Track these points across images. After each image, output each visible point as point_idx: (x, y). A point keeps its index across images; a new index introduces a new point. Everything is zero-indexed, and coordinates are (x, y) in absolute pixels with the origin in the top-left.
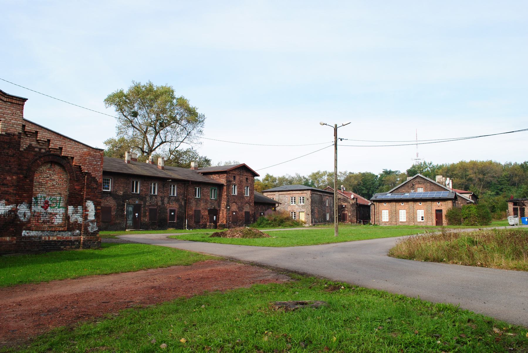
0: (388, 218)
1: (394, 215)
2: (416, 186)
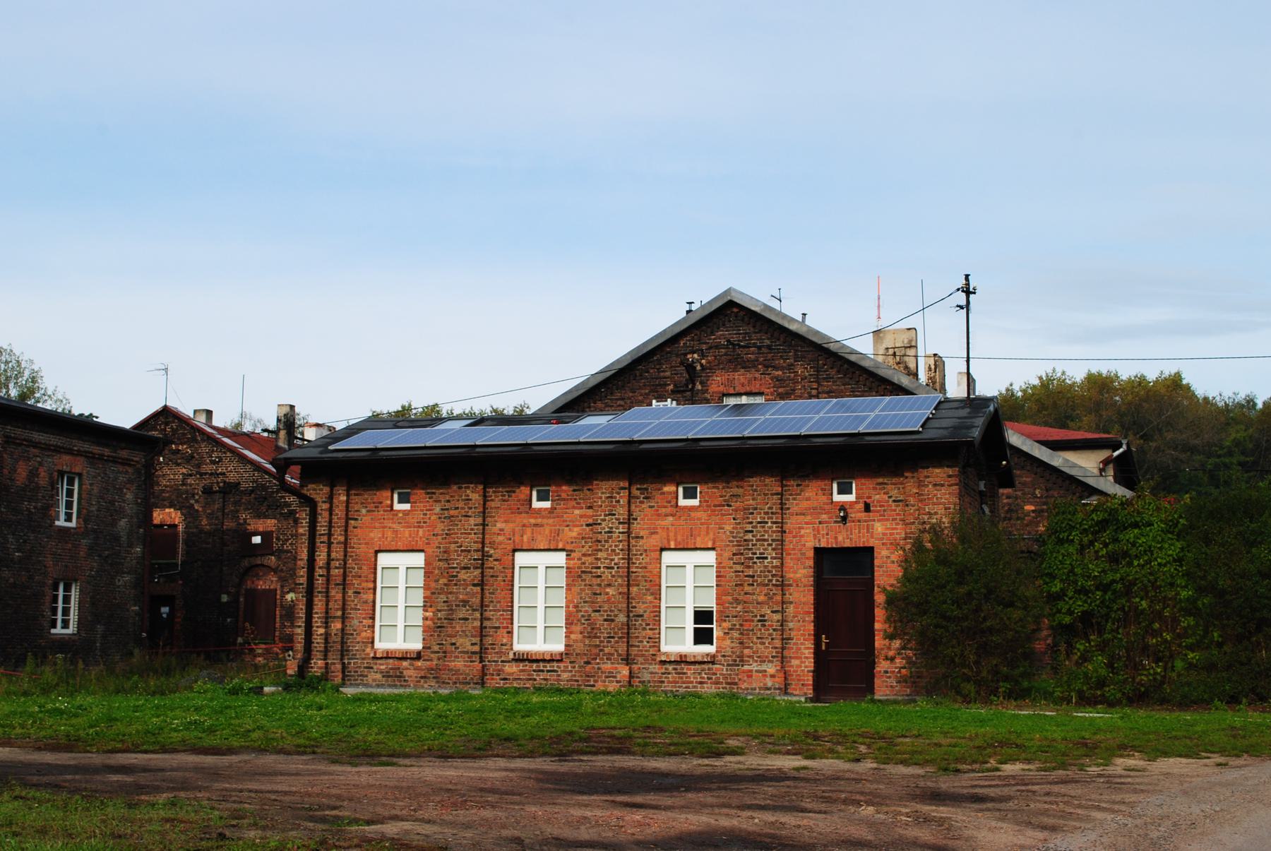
0: (417, 617)
1: (471, 594)
2: (717, 382)
